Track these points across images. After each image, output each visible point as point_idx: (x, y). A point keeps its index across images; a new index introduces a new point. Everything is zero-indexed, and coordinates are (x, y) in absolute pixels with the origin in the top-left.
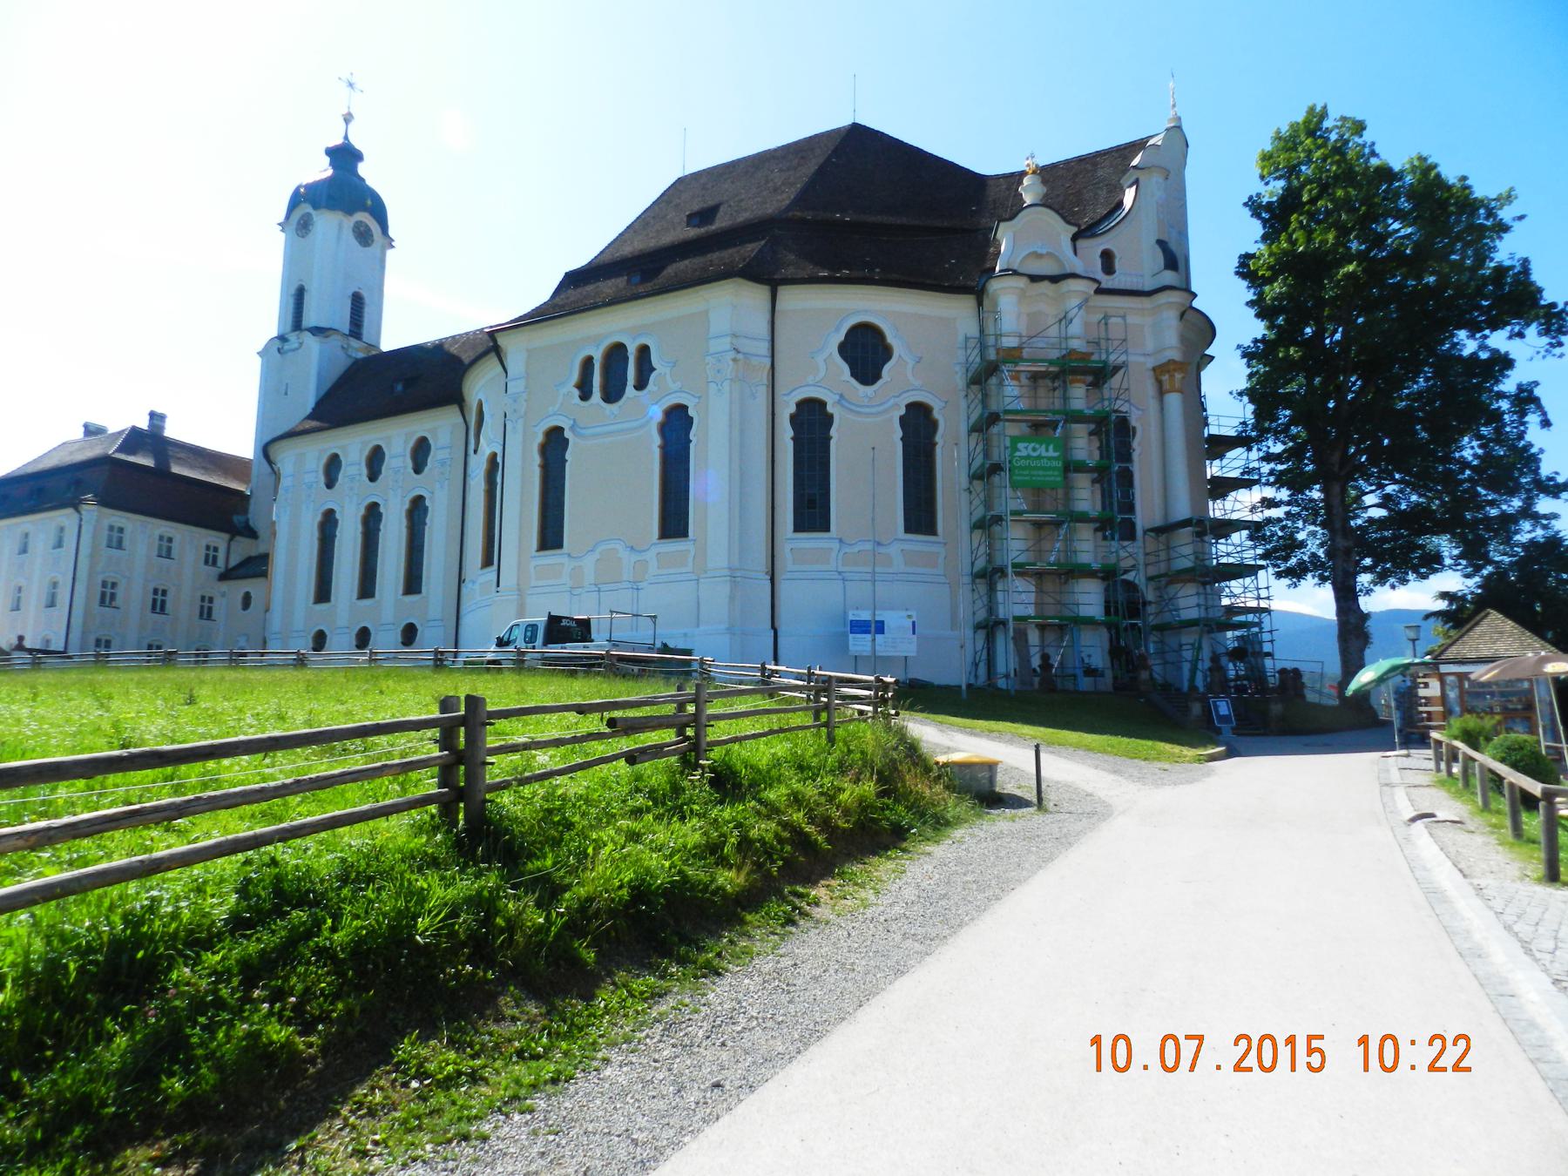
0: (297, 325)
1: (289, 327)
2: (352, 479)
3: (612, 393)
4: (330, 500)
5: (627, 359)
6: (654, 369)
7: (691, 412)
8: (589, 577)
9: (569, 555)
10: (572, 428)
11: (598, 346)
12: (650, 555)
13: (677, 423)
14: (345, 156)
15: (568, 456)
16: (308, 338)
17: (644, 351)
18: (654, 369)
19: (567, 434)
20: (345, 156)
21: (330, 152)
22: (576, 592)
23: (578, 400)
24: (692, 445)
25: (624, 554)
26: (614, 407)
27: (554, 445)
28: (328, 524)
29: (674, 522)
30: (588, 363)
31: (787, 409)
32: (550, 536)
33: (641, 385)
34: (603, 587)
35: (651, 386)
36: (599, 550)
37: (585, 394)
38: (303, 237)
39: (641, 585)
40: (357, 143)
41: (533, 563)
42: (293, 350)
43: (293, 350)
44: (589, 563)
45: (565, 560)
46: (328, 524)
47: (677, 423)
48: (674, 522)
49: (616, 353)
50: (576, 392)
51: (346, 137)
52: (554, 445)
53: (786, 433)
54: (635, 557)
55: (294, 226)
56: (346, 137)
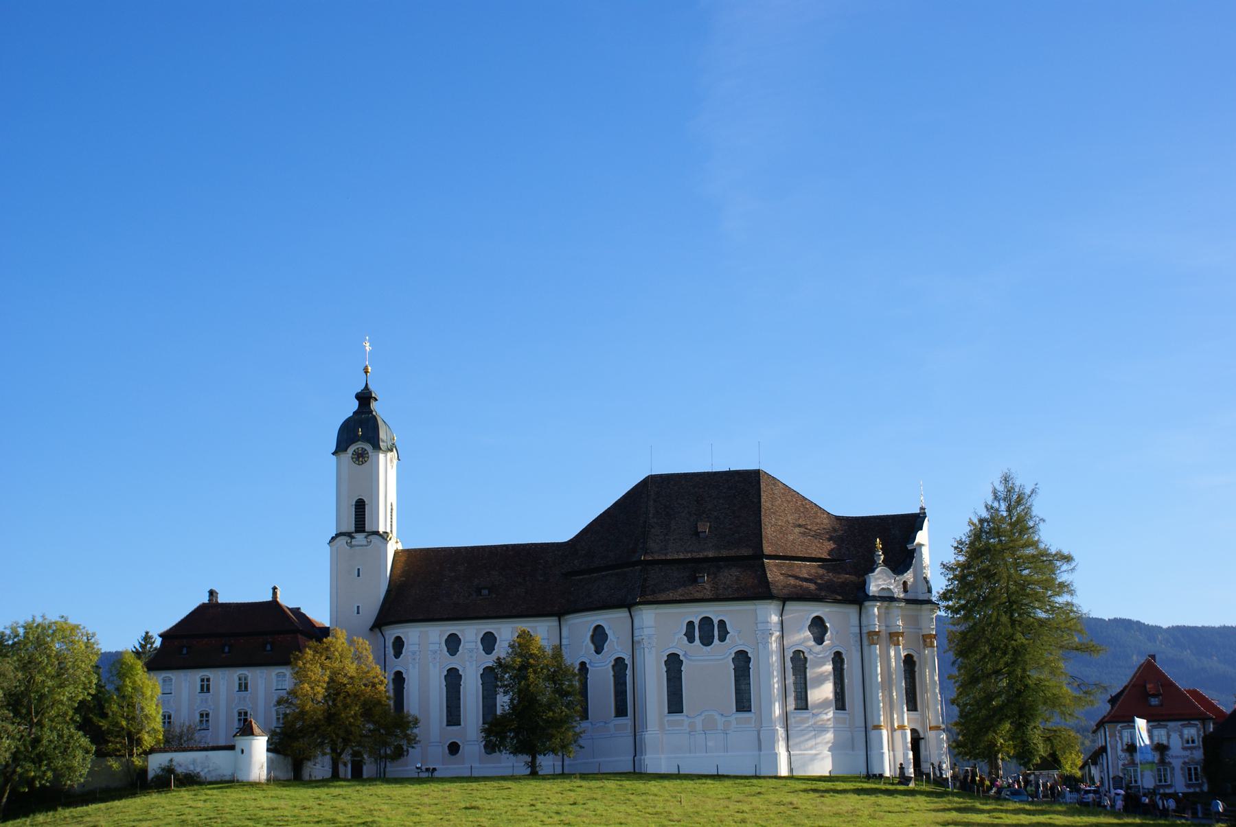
0: (360, 525)
1: (352, 529)
2: (471, 651)
3: (707, 640)
4: (454, 662)
5: (714, 626)
6: (728, 633)
7: (749, 655)
8: (699, 727)
9: (687, 716)
10: (684, 655)
11: (696, 618)
12: (734, 717)
13: (742, 662)
14: (365, 398)
15: (682, 669)
16: (374, 539)
17: (722, 623)
18: (728, 633)
19: (682, 658)
20: (365, 398)
21: (358, 397)
22: (692, 733)
23: (687, 642)
24: (751, 670)
25: (718, 717)
26: (708, 648)
27: (674, 664)
28: (453, 677)
29: (743, 703)
30: (691, 624)
31: (789, 655)
32: (675, 704)
33: (722, 639)
34: (707, 732)
35: (727, 640)
36: (703, 715)
37: (691, 639)
38: (359, 464)
39: (728, 732)
40: (375, 390)
41: (666, 719)
42: (362, 546)
43: (362, 546)
44: (699, 721)
45: (685, 718)
46: (453, 677)
47: (742, 662)
48: (743, 703)
49: (706, 621)
50: (685, 638)
51: (367, 384)
52: (674, 664)
53: (789, 664)
54: (724, 719)
55: (350, 455)
56: (367, 384)
